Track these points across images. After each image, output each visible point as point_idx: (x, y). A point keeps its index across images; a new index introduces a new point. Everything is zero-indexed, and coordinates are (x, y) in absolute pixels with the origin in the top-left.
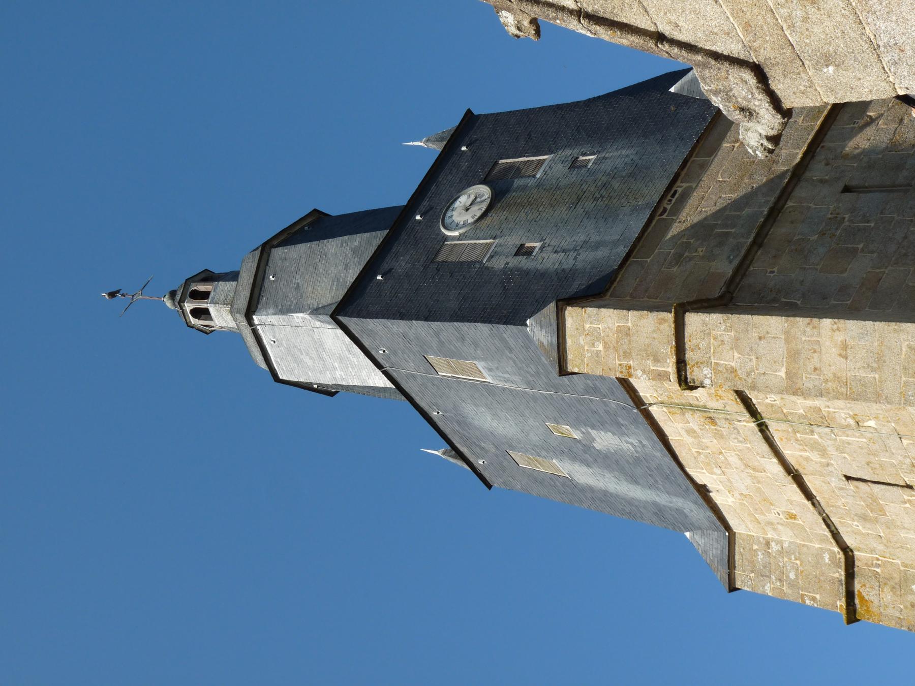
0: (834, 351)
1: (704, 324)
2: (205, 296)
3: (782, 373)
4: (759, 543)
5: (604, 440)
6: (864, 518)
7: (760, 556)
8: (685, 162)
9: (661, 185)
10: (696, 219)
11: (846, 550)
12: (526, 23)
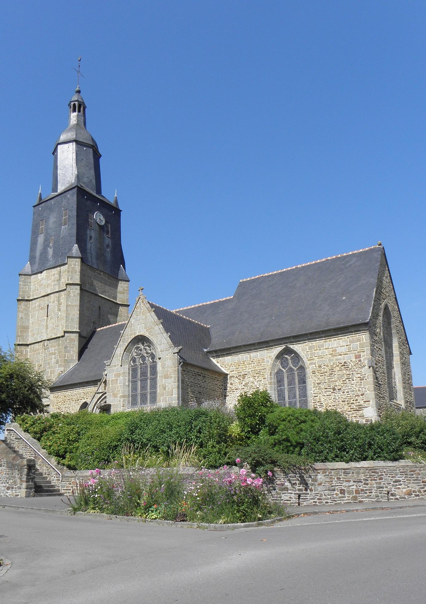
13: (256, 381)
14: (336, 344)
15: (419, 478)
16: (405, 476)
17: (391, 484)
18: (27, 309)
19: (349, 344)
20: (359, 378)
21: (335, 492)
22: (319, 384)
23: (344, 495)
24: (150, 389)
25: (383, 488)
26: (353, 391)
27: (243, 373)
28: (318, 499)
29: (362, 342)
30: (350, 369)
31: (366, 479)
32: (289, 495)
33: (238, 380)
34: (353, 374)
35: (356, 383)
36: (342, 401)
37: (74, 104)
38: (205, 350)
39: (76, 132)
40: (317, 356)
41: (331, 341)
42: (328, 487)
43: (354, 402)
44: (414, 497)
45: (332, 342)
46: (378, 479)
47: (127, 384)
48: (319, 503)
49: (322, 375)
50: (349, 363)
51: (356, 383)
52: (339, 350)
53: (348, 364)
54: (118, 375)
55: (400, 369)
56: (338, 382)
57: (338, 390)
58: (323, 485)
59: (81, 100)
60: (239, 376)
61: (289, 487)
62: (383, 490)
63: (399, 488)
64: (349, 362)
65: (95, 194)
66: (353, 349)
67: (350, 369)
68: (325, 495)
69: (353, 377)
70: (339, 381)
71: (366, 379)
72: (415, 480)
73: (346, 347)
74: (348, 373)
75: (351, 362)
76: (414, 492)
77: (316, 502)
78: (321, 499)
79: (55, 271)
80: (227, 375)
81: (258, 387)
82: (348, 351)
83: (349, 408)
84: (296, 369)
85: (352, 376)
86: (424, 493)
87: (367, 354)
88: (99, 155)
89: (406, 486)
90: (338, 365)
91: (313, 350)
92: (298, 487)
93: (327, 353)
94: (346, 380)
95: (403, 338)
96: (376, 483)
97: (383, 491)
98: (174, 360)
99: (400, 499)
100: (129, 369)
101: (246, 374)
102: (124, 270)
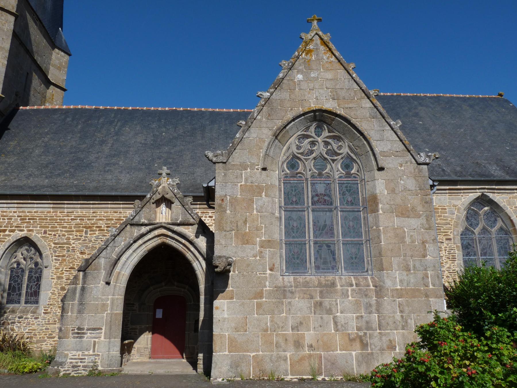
1: (10, 22)
8: (44, 27)
9: (40, 17)
10: (30, 25)
12: (241, 125)
24: (344, 236)
47: (277, 214)
98: (420, 179)
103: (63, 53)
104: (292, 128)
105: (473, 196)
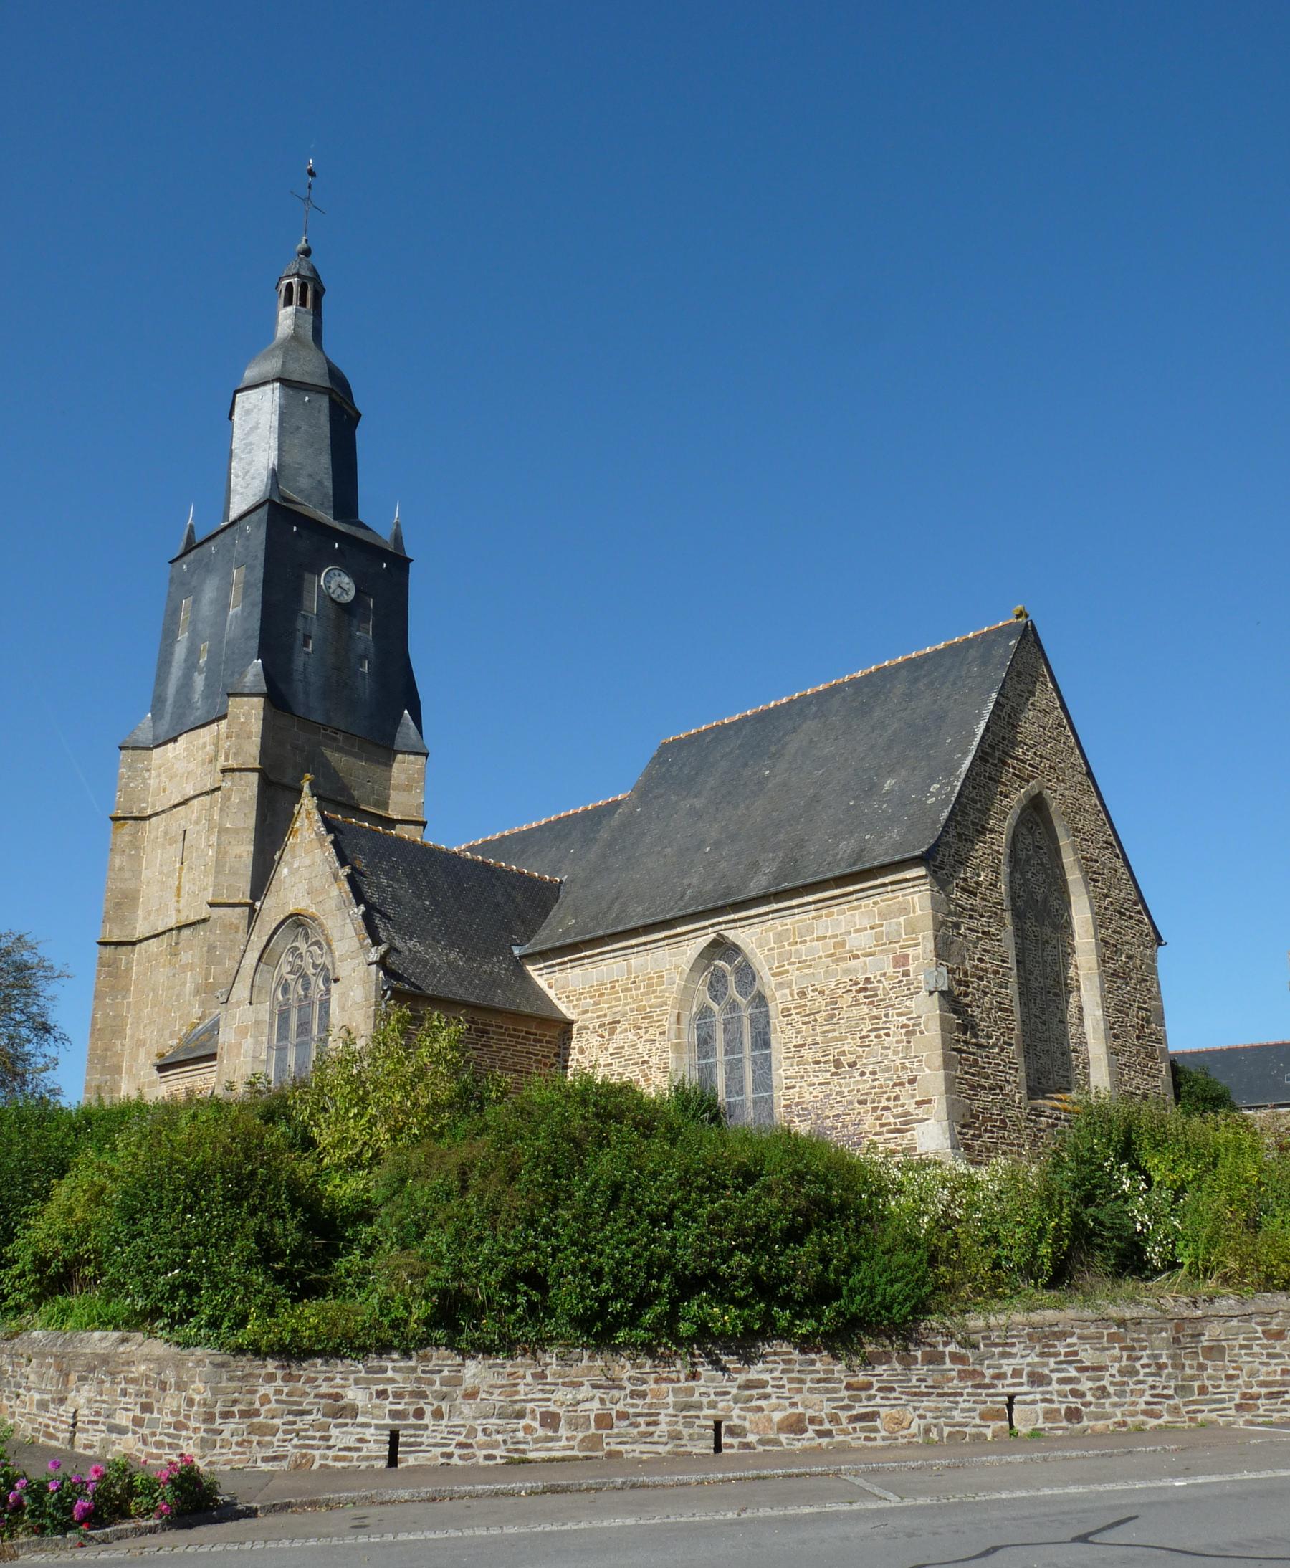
0: (238, 852)
2: (303, 303)
3: (228, 826)
4: (148, 765)
5: (199, 680)
6: (166, 833)
7: (141, 766)
11: (149, 817)
13: (642, 1040)
14: (843, 924)
15: (836, 1375)
16: (782, 1366)
17: (728, 1393)
18: (135, 844)
19: (877, 922)
20: (903, 1026)
21: (522, 1422)
22: (799, 1047)
23: (556, 1431)
25: (699, 1407)
26: (887, 1069)
27: (609, 1019)
28: (461, 1445)
29: (912, 915)
30: (881, 1000)
31: (638, 1379)
32: (359, 1430)
33: (599, 1039)
34: (886, 1015)
35: (897, 1042)
36: (860, 1102)
37: (289, 286)
38: (517, 951)
39: (284, 357)
40: (794, 963)
41: (831, 914)
42: (498, 1404)
43: (891, 1104)
44: (812, 1439)
45: (835, 917)
46: (682, 1377)
47: (263, 1057)
48: (461, 1457)
49: (807, 1019)
50: (879, 981)
51: (897, 1042)
52: (854, 942)
53: (876, 984)
54: (242, 1032)
55: (1097, 992)
56: (850, 1041)
57: (850, 1066)
58: (482, 1400)
59: (308, 273)
60: (600, 1026)
61: (360, 1404)
62: (701, 1414)
63: (760, 1409)
64: (879, 978)
65: (327, 518)
66: (888, 939)
67: (881, 1000)
68: (484, 1431)
69: (887, 1025)
70: (853, 1039)
71: (922, 1032)
72: (819, 1381)
73: (869, 931)
74: (874, 1012)
75: (883, 979)
76: (812, 1420)
77: (450, 1456)
78: (470, 1446)
79: (206, 735)
80: (571, 1023)
81: (646, 1058)
82: (875, 946)
83: (878, 1122)
84: (745, 1002)
85: (884, 1022)
86: (850, 1427)
87: (924, 951)
88: (353, 414)
89: (786, 1402)
90: (848, 988)
91: (786, 943)
92: (391, 1403)
93: (821, 954)
94: (868, 1036)
95: (1123, 895)
96: (675, 1391)
97: (698, 1417)
99: (760, 1448)
100: (272, 1012)
101: (618, 1022)
102: (412, 724)
103: (412, 757)
104: (277, 943)
105: (703, 941)
